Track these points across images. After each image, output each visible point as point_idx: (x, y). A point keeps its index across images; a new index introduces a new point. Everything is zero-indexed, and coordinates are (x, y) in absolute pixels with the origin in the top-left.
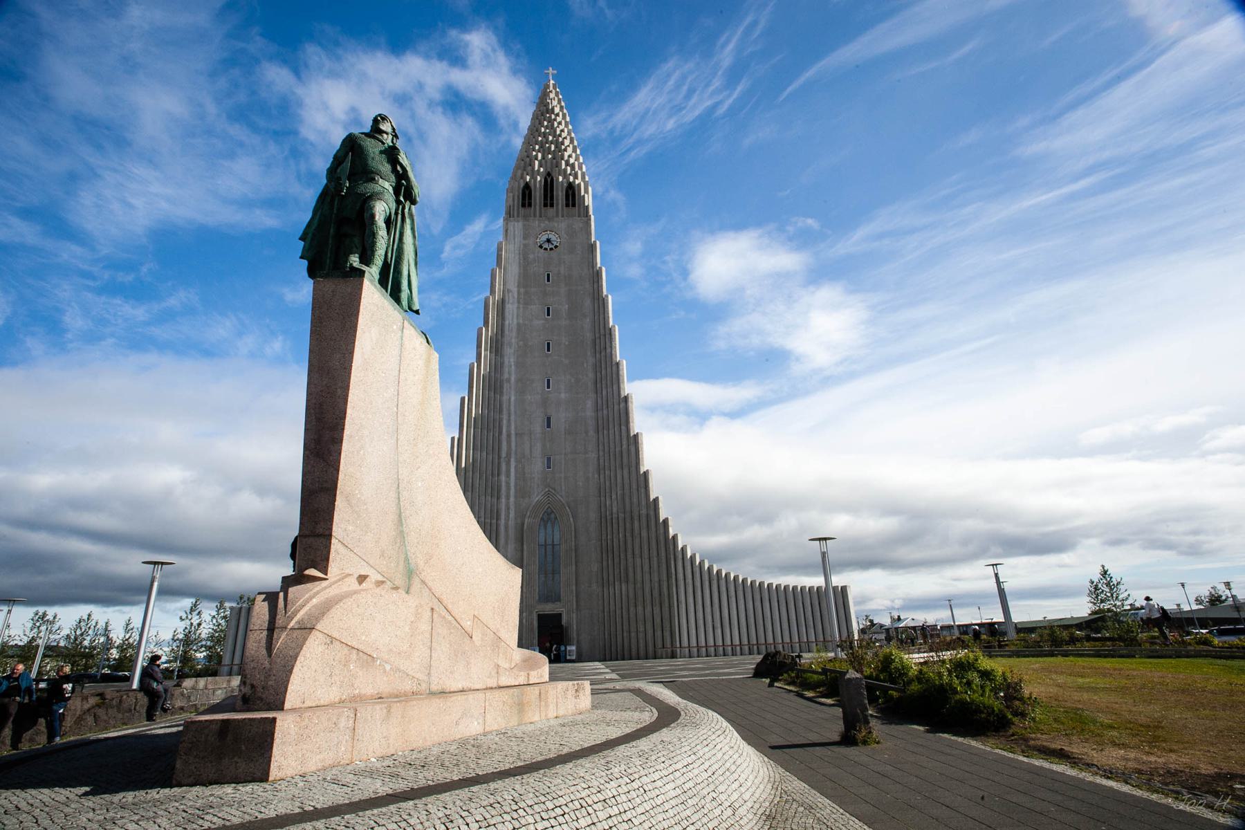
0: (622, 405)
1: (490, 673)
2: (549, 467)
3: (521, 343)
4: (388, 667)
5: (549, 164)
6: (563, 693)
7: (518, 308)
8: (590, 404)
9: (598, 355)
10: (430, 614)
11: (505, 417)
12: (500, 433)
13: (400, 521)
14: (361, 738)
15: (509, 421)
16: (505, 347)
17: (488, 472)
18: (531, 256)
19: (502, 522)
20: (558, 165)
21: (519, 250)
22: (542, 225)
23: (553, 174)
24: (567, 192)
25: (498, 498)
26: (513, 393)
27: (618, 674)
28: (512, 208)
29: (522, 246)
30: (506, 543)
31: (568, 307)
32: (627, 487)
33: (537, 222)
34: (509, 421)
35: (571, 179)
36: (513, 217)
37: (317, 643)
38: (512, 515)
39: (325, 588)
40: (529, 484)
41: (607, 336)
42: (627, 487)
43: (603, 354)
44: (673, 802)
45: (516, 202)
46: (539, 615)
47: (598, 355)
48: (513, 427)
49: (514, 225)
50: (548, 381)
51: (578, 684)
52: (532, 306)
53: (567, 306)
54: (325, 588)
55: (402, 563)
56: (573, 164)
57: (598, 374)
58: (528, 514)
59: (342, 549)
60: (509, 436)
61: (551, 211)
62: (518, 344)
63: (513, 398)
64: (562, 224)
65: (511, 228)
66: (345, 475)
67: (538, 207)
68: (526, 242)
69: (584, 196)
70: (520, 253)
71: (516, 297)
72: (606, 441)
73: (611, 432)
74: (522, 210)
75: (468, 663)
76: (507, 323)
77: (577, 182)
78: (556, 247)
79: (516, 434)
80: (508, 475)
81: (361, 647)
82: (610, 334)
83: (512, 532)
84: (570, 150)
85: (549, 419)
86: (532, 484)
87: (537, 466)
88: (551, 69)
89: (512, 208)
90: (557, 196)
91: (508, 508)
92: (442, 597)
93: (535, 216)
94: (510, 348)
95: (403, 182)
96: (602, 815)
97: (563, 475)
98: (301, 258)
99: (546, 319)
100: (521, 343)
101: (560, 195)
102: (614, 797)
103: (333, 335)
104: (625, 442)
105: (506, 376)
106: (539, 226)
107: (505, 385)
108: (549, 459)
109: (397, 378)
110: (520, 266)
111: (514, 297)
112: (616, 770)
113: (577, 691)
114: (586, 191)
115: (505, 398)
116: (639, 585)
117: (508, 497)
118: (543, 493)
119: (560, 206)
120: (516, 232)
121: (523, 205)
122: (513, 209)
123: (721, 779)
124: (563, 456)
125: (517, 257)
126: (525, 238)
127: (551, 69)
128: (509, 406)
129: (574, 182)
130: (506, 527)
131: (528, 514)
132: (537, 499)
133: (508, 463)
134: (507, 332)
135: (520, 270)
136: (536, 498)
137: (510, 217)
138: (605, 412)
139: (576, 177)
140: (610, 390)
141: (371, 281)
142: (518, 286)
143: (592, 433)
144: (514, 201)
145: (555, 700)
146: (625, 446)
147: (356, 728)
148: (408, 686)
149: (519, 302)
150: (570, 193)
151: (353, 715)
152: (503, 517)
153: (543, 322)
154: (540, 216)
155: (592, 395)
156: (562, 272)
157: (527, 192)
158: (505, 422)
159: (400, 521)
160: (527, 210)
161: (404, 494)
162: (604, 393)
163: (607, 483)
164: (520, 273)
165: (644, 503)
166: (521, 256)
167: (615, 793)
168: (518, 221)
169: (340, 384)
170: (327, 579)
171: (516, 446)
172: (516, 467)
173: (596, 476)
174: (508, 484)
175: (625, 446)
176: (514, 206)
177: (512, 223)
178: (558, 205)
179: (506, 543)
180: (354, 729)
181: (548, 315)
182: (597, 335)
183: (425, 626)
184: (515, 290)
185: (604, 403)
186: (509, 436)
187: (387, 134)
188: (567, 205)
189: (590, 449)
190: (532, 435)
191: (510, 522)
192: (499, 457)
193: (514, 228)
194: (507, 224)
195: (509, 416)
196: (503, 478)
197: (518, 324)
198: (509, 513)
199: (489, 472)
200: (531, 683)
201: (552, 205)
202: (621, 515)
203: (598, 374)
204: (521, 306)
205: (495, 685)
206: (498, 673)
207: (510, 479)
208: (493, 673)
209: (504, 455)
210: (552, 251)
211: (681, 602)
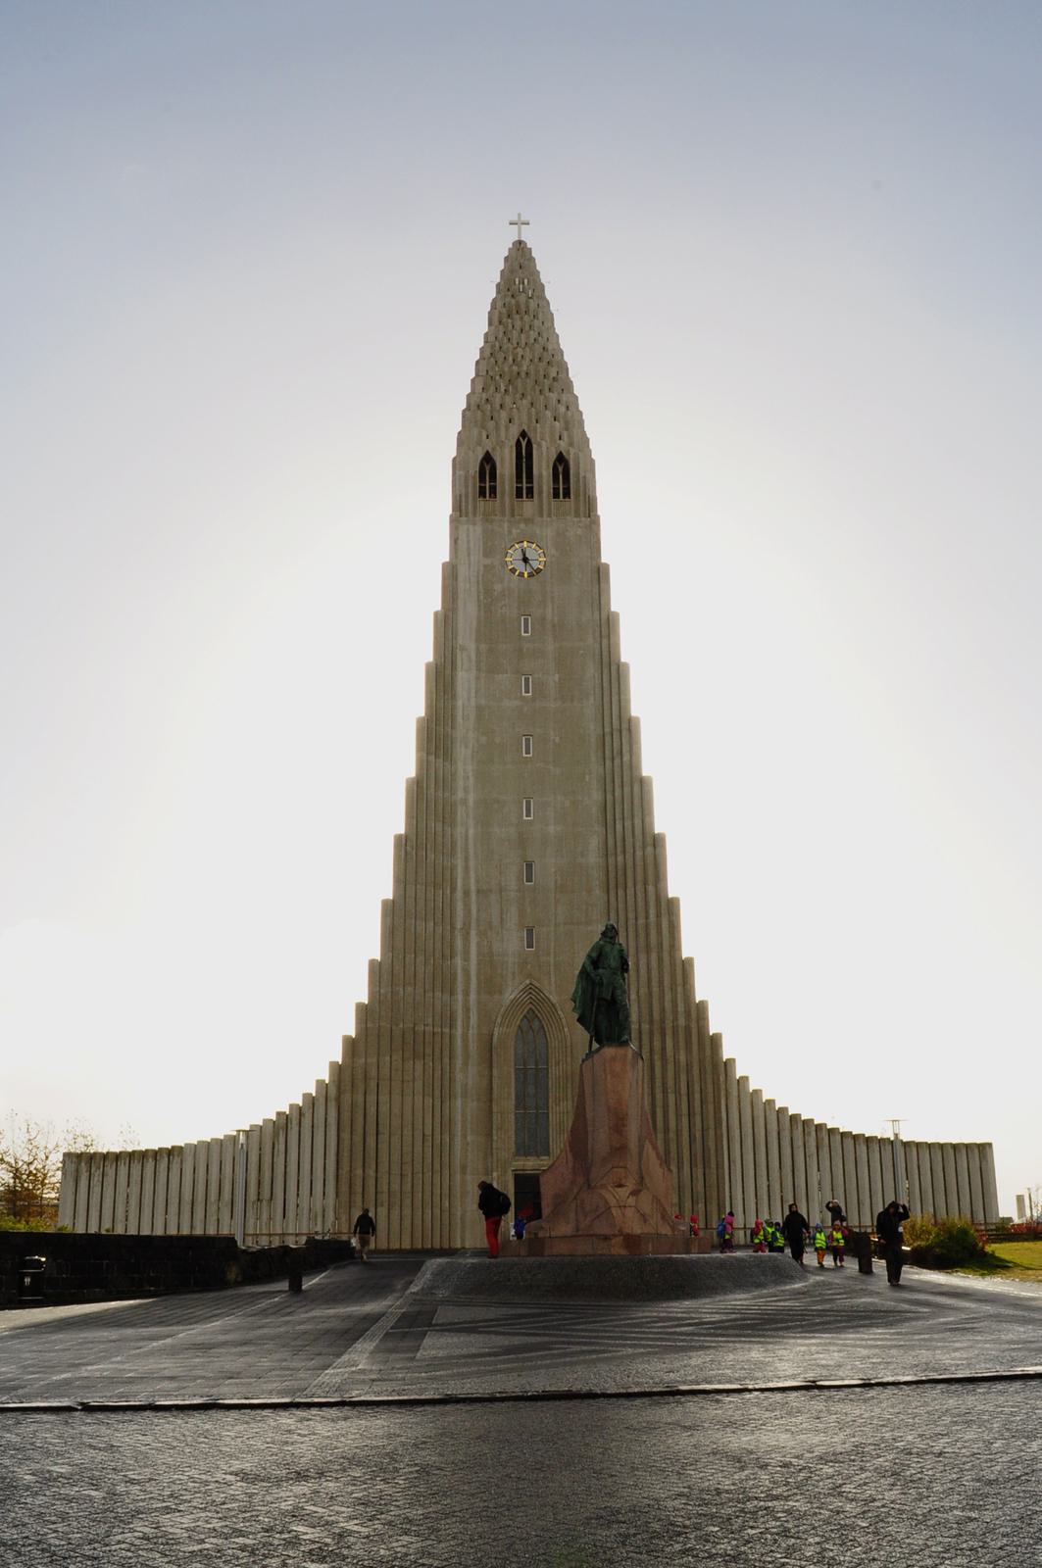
0: (650, 849)
2: (530, 945)
3: (484, 739)
5: (525, 419)
7: (478, 678)
8: (594, 843)
9: (608, 763)
11: (460, 863)
12: (453, 890)
15: (466, 869)
16: (458, 744)
17: (437, 956)
18: (498, 587)
19: (459, 1031)
21: (478, 577)
23: (531, 435)
24: (555, 468)
25: (452, 993)
26: (471, 822)
28: (463, 499)
29: (482, 568)
30: (466, 1064)
31: (560, 679)
32: (655, 983)
33: (506, 525)
34: (466, 869)
38: (474, 1020)
40: (499, 971)
41: (624, 733)
42: (655, 983)
43: (617, 761)
45: (470, 490)
47: (608, 763)
48: (472, 881)
49: (468, 530)
50: (528, 803)
53: (557, 675)
57: (609, 797)
58: (499, 1020)
60: (467, 893)
61: (528, 507)
62: (478, 741)
63: (471, 832)
64: (547, 531)
65: (463, 537)
67: (507, 499)
68: (488, 561)
69: (585, 477)
71: (474, 658)
72: (621, 906)
73: (631, 891)
74: (481, 503)
76: (460, 703)
77: (572, 451)
78: (538, 571)
79: (478, 891)
80: (466, 958)
82: (630, 730)
83: (473, 1047)
85: (529, 866)
87: (511, 943)
89: (463, 499)
90: (540, 476)
91: (467, 1009)
93: (503, 514)
94: (466, 747)
97: (552, 961)
101: (543, 469)
104: (652, 911)
105: (460, 794)
106: (510, 532)
107: (459, 807)
108: (530, 932)
110: (479, 606)
111: (470, 661)
115: (460, 830)
116: (672, 1135)
117: (466, 993)
118: (522, 987)
119: (545, 495)
120: (472, 545)
121: (482, 493)
122: (467, 502)
124: (552, 929)
125: (474, 589)
128: (466, 844)
131: (499, 1020)
132: (512, 997)
134: (460, 720)
135: (479, 611)
136: (510, 995)
137: (461, 516)
138: (620, 858)
139: (571, 444)
140: (628, 823)
142: (476, 640)
143: (598, 892)
144: (467, 487)
146: (652, 918)
149: (479, 669)
150: (560, 469)
152: (459, 1023)
153: (518, 703)
155: (598, 829)
156: (549, 616)
157: (488, 468)
158: (460, 870)
162: (619, 827)
164: (479, 617)
165: (681, 1008)
166: (481, 586)
168: (475, 524)
171: (478, 911)
172: (478, 944)
174: (466, 972)
175: (652, 918)
176: (467, 496)
177: (465, 527)
178: (540, 493)
179: (466, 1064)
181: (527, 691)
182: (607, 730)
184: (472, 646)
185: (619, 844)
186: (467, 893)
188: (556, 495)
189: (595, 918)
191: (470, 1032)
193: (468, 536)
194: (457, 528)
195: (466, 859)
196: (459, 961)
197: (479, 708)
198: (469, 1018)
199: (438, 955)
201: (530, 493)
202: (645, 1027)
203: (609, 797)
207: (468, 964)
209: (459, 925)
210: (532, 579)
211: (734, 1162)
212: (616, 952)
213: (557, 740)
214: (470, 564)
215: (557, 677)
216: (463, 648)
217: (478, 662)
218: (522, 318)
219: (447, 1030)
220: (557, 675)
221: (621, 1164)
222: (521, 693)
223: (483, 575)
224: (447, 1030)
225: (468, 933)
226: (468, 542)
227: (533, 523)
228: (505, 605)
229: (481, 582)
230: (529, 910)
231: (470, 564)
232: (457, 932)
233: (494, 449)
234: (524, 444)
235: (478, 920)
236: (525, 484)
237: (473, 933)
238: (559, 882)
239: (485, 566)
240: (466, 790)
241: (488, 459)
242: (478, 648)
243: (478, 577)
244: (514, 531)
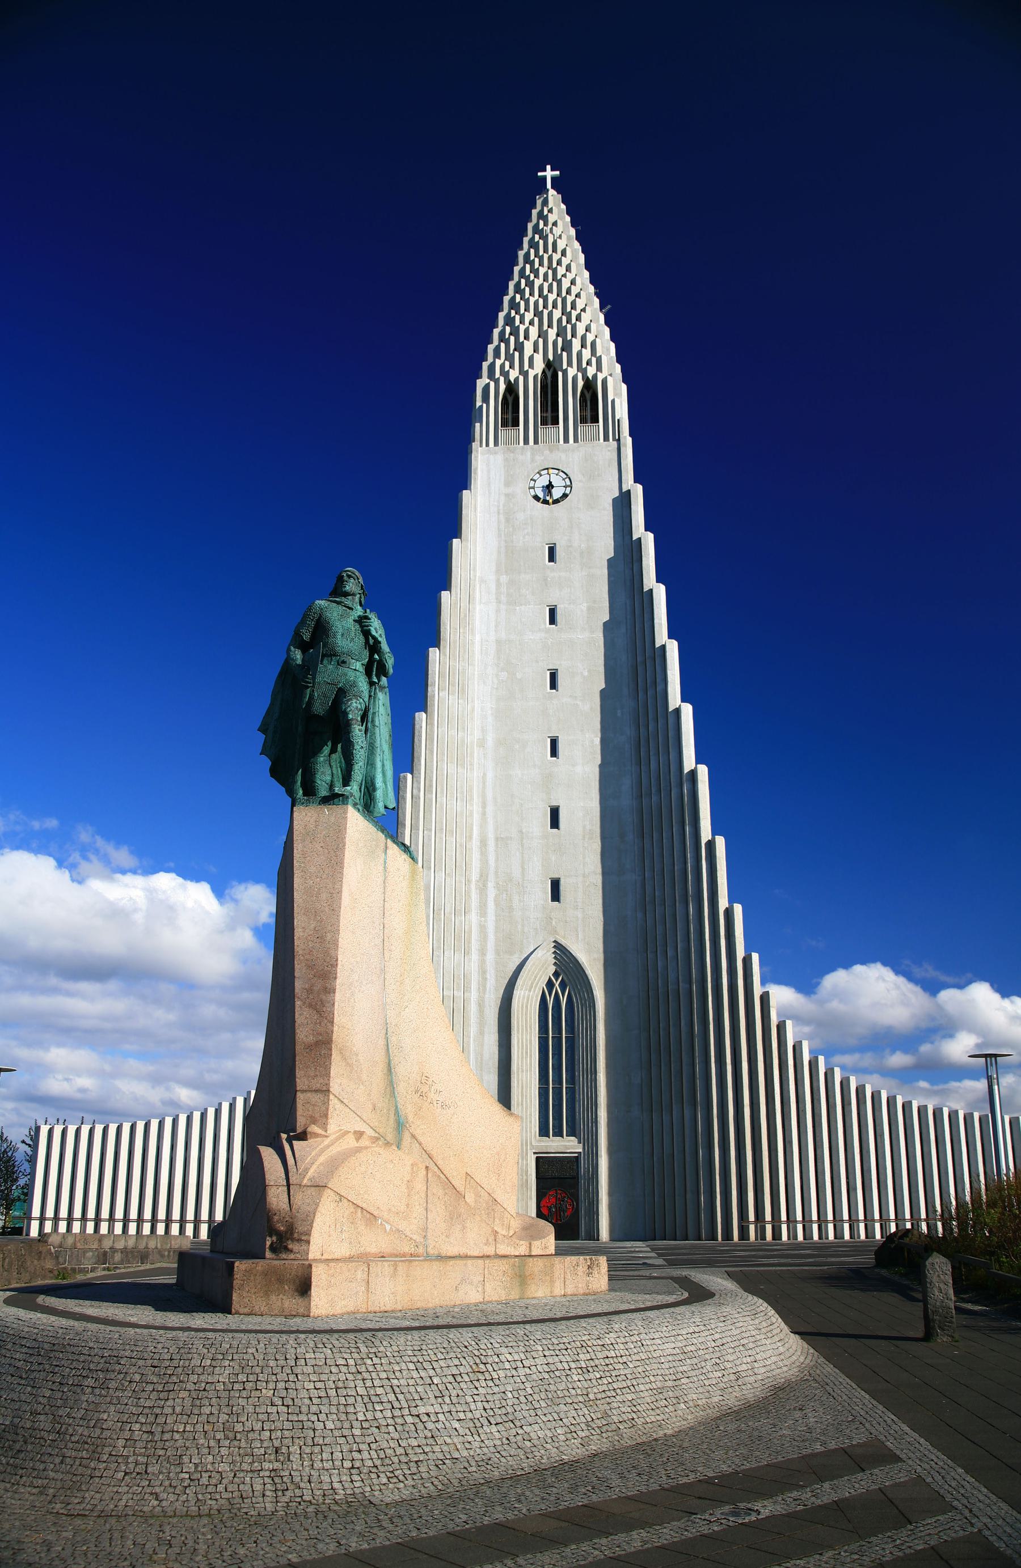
1: (487, 1240)
4: (388, 1227)
6: (572, 1269)
7: (498, 611)
10: (425, 1173)
13: (389, 1069)
14: (374, 1291)
15: (484, 814)
18: (521, 516)
19: (474, 995)
20: (567, 347)
22: (538, 458)
23: (557, 365)
25: (467, 953)
27: (656, 1253)
29: (503, 498)
31: (589, 609)
33: (529, 454)
35: (591, 371)
36: (487, 445)
37: (329, 1200)
39: (328, 1146)
44: (670, 1358)
46: (537, 1159)
51: (591, 1259)
52: (523, 608)
53: (585, 605)
54: (328, 1146)
55: (392, 1116)
56: (593, 344)
59: (338, 1105)
60: (483, 843)
63: (490, 775)
66: (339, 1027)
69: (613, 401)
70: (499, 513)
71: (494, 591)
75: (464, 1227)
76: (478, 638)
77: (600, 377)
79: (497, 839)
81: (364, 1206)
84: (586, 318)
86: (526, 929)
88: (548, 167)
91: (483, 972)
92: (432, 1153)
93: (526, 441)
95: (376, 656)
96: (600, 1355)
98: (261, 754)
99: (547, 631)
100: (504, 675)
102: (612, 1344)
106: (533, 460)
109: (382, 909)
110: (499, 536)
112: (617, 1326)
113: (589, 1267)
114: (618, 394)
117: (483, 952)
123: (731, 1350)
126: (507, 484)
127: (548, 167)
129: (595, 376)
130: (481, 1006)
133: (483, 890)
138: (654, 798)
139: (599, 368)
141: (355, 805)
145: (562, 1276)
147: (370, 1281)
148: (407, 1248)
149: (498, 601)
151: (366, 1269)
152: (474, 986)
154: (536, 442)
159: (389, 1069)
160: (511, 431)
161: (393, 1039)
163: (659, 929)
166: (502, 517)
167: (614, 1342)
169: (329, 928)
170: (326, 1137)
171: (497, 860)
173: (640, 915)
174: (483, 928)
179: (481, 1032)
180: (368, 1282)
183: (420, 1186)
187: (354, 595)
190: (524, 841)
191: (487, 996)
192: (468, 882)
195: (484, 805)
196: (474, 917)
197: (498, 642)
198: (486, 979)
200: (533, 1254)
204: (503, 607)
205: (492, 1253)
206: (495, 1240)
207: (486, 921)
208: (490, 1240)
212: (350, 623)
213: (586, 674)
214: (490, 493)
215: (584, 606)
216: (482, 581)
217: (498, 593)
218: (550, 258)
219: (460, 994)
220: (585, 605)
221: (316, 1084)
222: (546, 624)
223: (504, 506)
224: (460, 994)
225: (485, 885)
226: (489, 471)
227: (558, 449)
228: (528, 534)
229: (501, 511)
230: (553, 859)
231: (490, 493)
232: (473, 886)
233: (517, 379)
234: (549, 374)
235: (496, 873)
236: (549, 414)
237: (490, 885)
238: (588, 827)
239: (507, 495)
240: (484, 731)
241: (511, 389)
242: (498, 580)
243: (499, 506)
244: (538, 458)
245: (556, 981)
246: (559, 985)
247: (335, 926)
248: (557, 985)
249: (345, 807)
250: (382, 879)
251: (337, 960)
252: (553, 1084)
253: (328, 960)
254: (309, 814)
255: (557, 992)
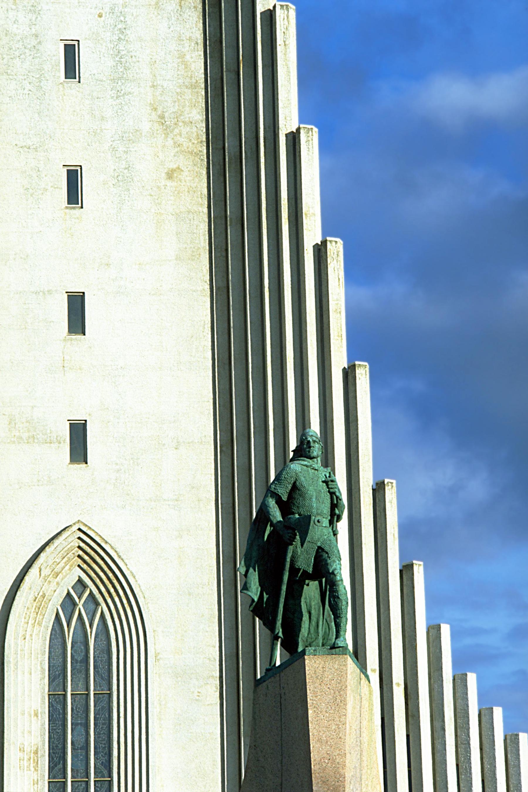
103: (328, 708)
245: (80, 598)
246: (83, 605)
247: (342, 751)
248: (80, 606)
249: (345, 656)
250: (359, 705)
251: (344, 778)
252: (73, 777)
253: (338, 776)
254: (318, 662)
255: (80, 614)
